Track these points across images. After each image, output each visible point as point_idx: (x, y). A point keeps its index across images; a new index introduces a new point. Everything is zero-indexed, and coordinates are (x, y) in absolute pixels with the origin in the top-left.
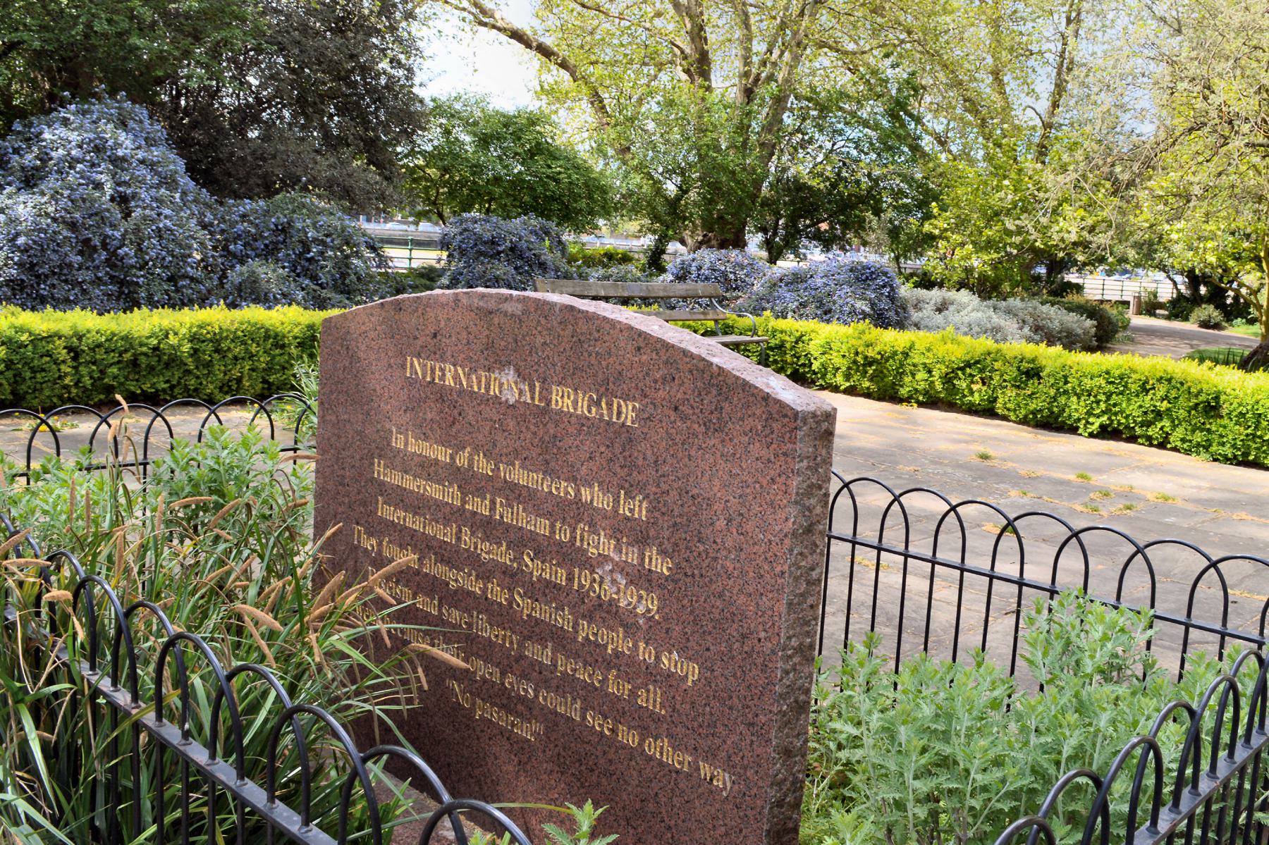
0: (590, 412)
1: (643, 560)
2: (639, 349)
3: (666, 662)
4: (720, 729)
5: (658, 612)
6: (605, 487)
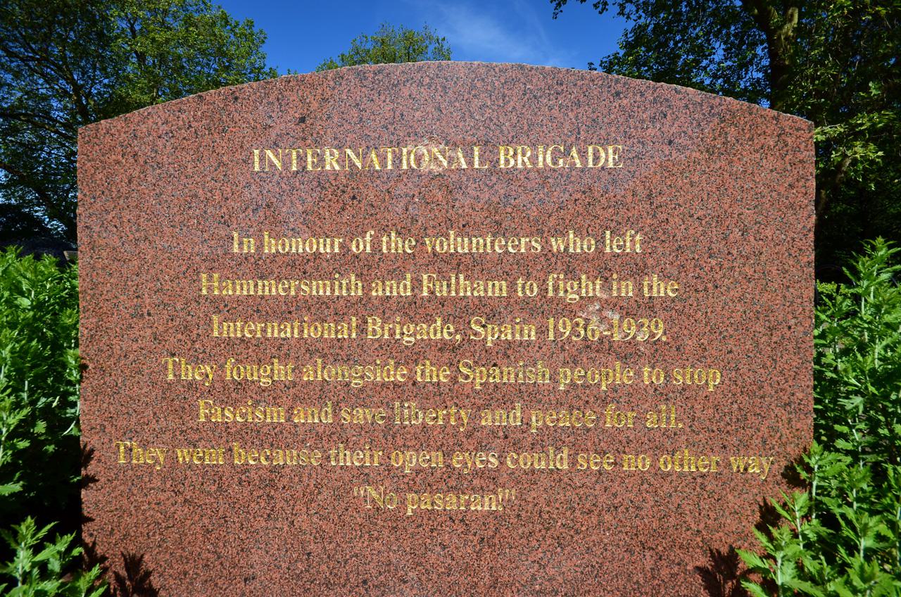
1: (641, 290)
2: (618, 94)
4: (752, 418)
5: (665, 333)
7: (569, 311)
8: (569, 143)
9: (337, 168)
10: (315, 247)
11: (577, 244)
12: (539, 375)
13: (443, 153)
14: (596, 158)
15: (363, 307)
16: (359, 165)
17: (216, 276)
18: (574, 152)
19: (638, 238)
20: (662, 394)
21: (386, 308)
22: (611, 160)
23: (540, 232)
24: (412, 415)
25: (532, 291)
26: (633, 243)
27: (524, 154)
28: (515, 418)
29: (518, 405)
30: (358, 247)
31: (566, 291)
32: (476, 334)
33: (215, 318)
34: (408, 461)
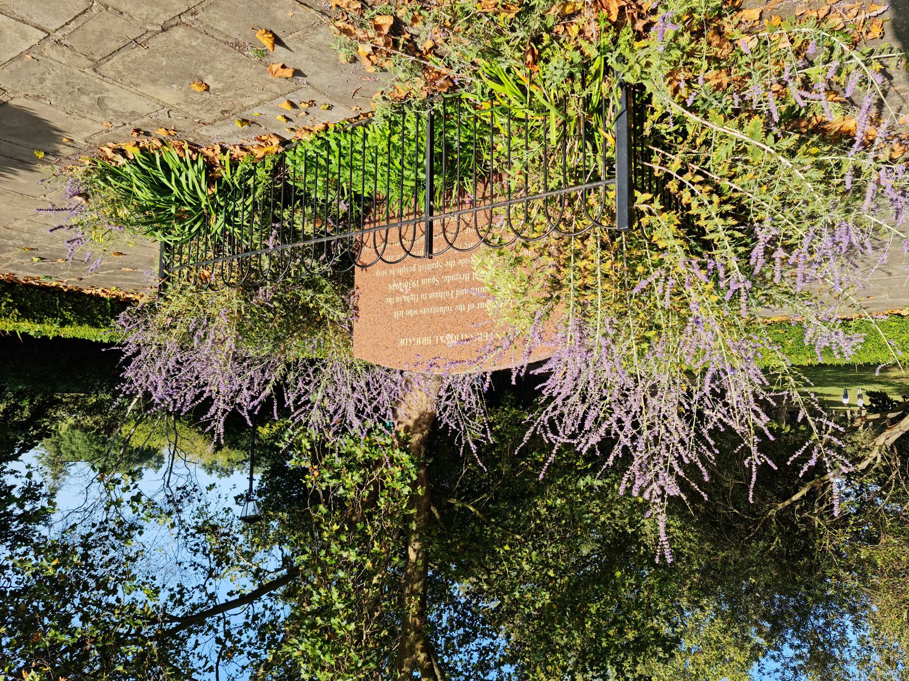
7: (413, 290)
26: (397, 314)
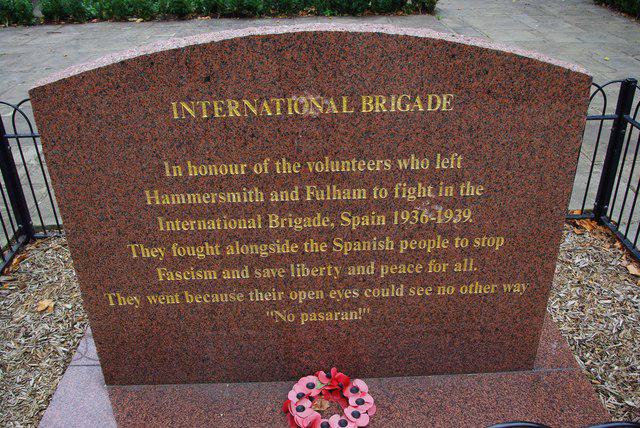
0: (404, 108)
1: (459, 192)
2: (453, 56)
3: (478, 243)
4: (519, 263)
5: (471, 217)
6: (420, 155)
7: (405, 205)
8: (415, 92)
9: (238, 115)
10: (227, 171)
11: (416, 164)
12: (388, 245)
13: (319, 101)
14: (434, 104)
15: (266, 208)
16: (254, 111)
17: (156, 192)
18: (418, 100)
19: (460, 158)
20: (465, 253)
21: (282, 209)
22: (444, 105)
23: (389, 156)
24: (303, 271)
25: (383, 195)
26: (456, 161)
27: (381, 101)
28: (370, 270)
29: (373, 263)
30: (258, 169)
31: (407, 194)
32: (345, 222)
33: (160, 219)
34: (301, 296)
